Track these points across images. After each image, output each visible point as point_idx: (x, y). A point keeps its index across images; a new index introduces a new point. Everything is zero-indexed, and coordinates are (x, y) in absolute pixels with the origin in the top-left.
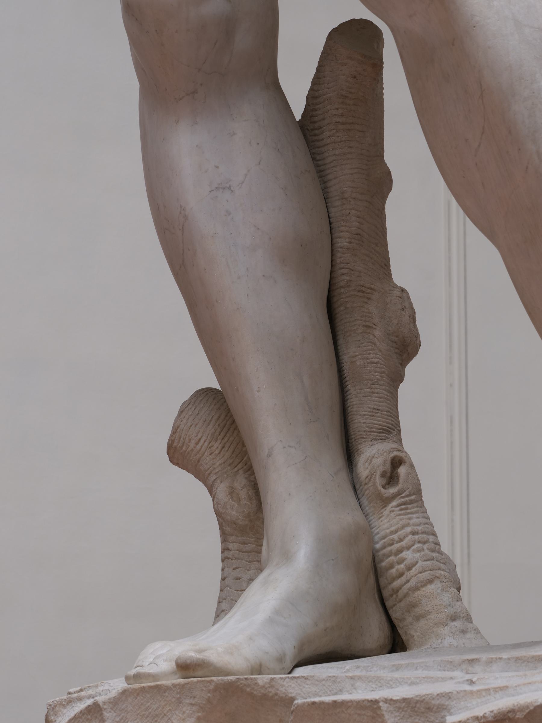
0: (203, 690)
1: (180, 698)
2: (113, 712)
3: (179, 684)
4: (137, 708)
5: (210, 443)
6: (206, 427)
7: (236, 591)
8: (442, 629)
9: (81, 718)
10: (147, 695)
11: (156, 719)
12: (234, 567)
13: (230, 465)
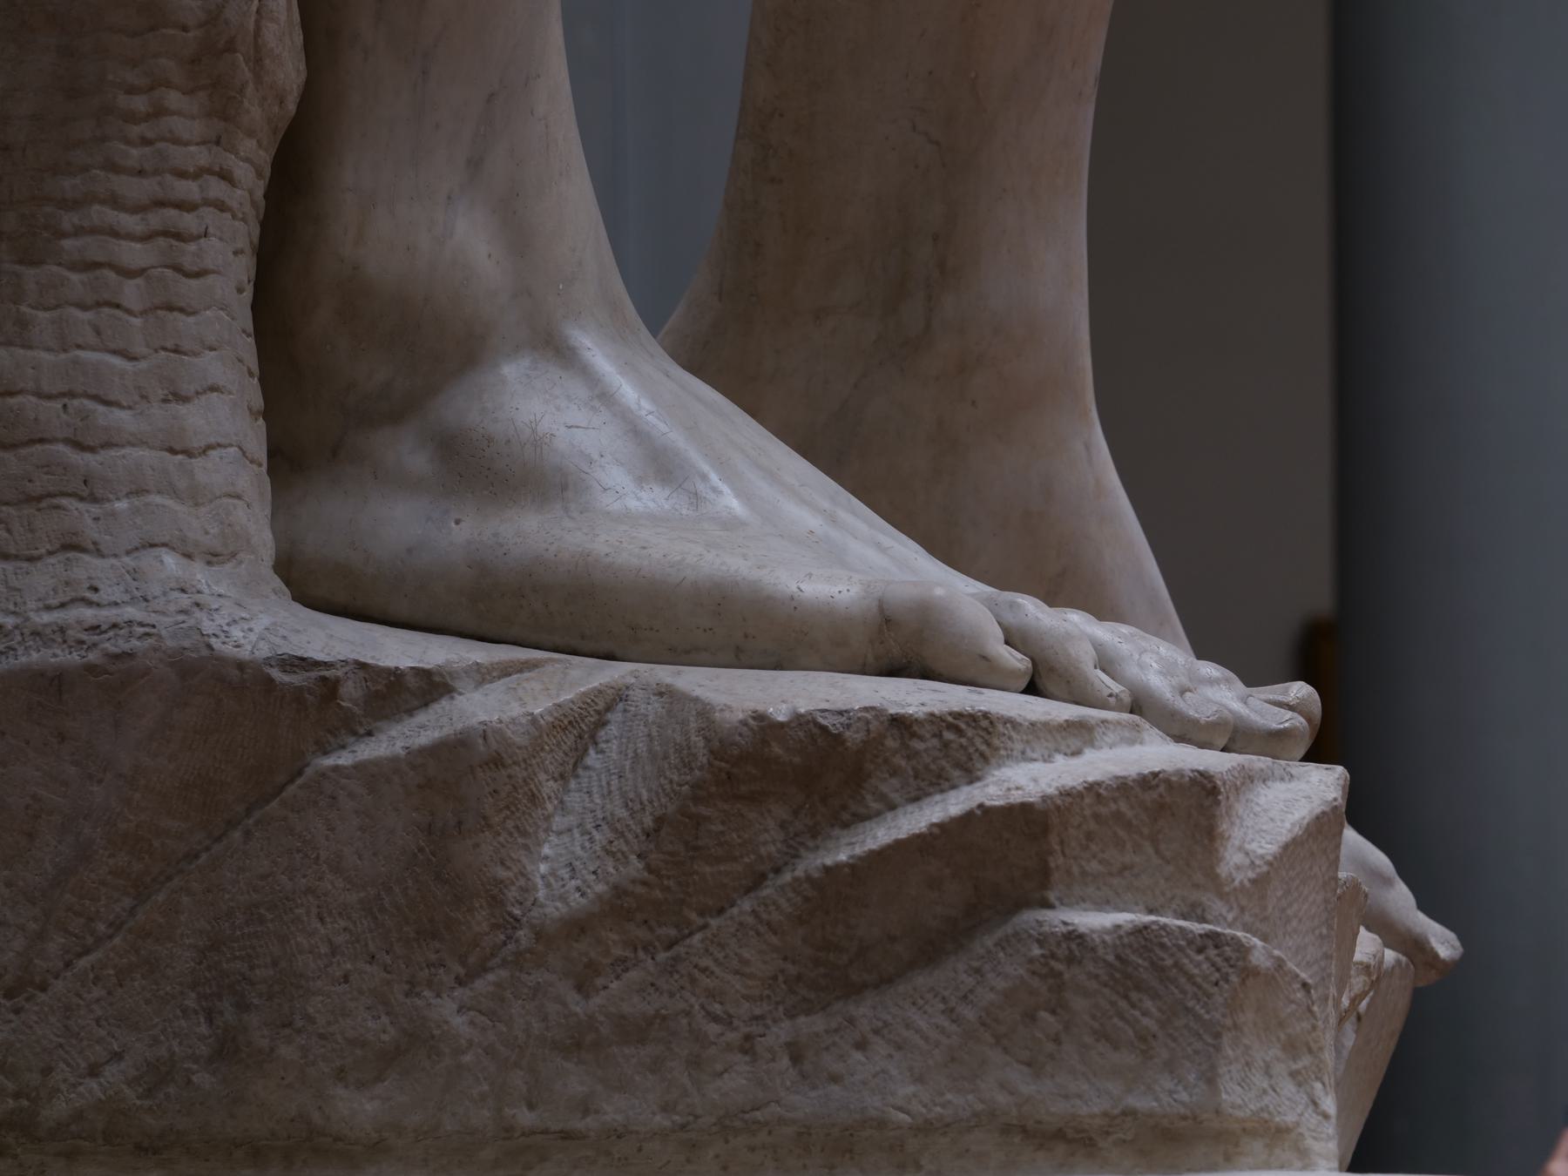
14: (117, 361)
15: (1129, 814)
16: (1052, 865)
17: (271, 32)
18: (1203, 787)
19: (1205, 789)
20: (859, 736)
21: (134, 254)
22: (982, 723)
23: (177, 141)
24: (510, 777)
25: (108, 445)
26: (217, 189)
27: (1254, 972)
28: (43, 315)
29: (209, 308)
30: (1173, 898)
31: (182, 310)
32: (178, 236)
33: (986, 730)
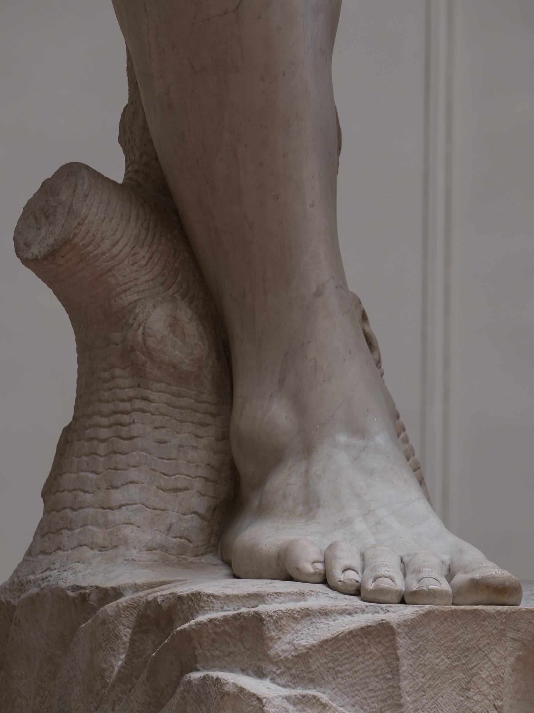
1: (504, 630)
2: (407, 638)
3: (505, 613)
5: (133, 248)
7: (161, 458)
9: (348, 640)
10: (458, 621)
11: (466, 654)
12: (157, 425)
13: (162, 284)
14: (91, 475)
15: (230, 631)
16: (197, 653)
17: (150, 342)
18: (257, 618)
21: (104, 433)
22: (196, 597)
23: (120, 388)
24: (108, 628)
25: (80, 508)
26: (138, 404)
27: (228, 694)
28: (77, 459)
29: (134, 451)
30: (251, 665)
31: (120, 453)
32: (122, 425)
33: (198, 599)
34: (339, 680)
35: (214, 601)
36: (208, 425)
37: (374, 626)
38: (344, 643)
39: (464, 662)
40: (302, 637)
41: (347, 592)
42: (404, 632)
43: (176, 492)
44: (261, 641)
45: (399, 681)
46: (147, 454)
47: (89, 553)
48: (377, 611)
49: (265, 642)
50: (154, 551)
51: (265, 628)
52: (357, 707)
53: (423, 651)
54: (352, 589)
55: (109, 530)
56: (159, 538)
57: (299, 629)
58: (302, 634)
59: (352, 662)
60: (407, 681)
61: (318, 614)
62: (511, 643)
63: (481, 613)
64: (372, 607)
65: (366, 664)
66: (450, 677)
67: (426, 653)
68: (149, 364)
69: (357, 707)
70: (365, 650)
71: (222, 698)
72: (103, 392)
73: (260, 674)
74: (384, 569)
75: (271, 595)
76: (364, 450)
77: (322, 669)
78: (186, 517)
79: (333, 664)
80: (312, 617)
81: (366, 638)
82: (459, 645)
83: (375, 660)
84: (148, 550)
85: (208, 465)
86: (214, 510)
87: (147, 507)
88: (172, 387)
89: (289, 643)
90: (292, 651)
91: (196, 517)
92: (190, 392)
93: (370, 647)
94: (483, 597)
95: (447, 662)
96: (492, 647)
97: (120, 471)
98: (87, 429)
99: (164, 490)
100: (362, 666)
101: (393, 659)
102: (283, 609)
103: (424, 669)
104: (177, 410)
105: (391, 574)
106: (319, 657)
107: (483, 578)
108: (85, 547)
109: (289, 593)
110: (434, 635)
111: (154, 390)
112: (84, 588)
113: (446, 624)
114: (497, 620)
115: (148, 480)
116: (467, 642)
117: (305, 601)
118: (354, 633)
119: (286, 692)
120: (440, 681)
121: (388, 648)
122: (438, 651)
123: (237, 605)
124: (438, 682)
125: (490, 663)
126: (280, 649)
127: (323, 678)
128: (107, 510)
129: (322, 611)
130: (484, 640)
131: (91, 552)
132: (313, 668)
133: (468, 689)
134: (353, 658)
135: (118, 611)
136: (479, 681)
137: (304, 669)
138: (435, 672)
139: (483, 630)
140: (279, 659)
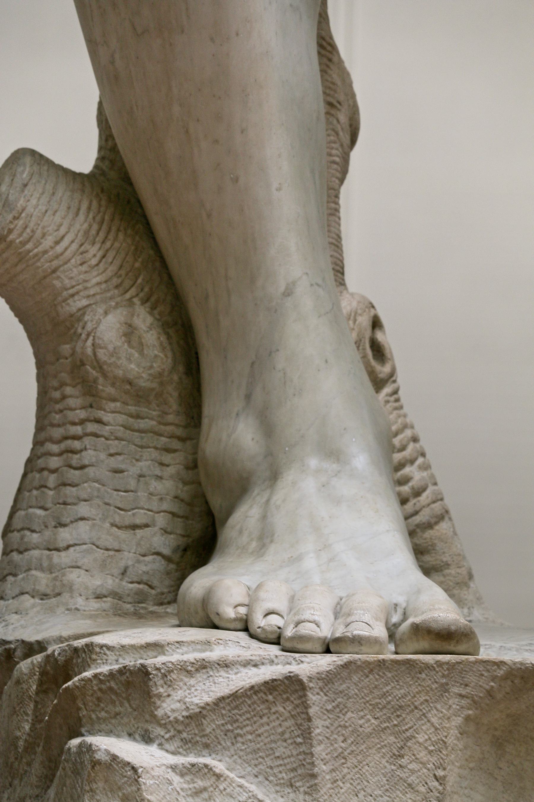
0: (482, 675)
1: (447, 684)
2: (322, 693)
3: (447, 663)
4: (366, 691)
5: (81, 245)
6: (74, 219)
7: (116, 490)
8: (466, 592)
9: (250, 697)
10: (387, 673)
11: (399, 713)
12: (112, 451)
13: (117, 287)
14: (40, 512)
15: (116, 687)
16: (81, 715)
17: (101, 354)
18: (143, 672)
19: (144, 672)
20: (63, 659)
23: (71, 409)
25: (26, 550)
26: (91, 427)
29: (86, 482)
30: (138, 728)
31: (70, 485)
32: (73, 452)
34: (239, 745)
35: (108, 652)
36: (175, 451)
37: (280, 680)
38: (245, 701)
39: (395, 722)
40: (196, 693)
41: (267, 640)
42: (318, 687)
43: (134, 530)
44: (148, 699)
45: (312, 746)
46: (100, 486)
47: (27, 601)
48: (289, 662)
49: (152, 700)
50: (105, 599)
51: (151, 683)
52: (261, 778)
53: (343, 709)
54: (273, 637)
55: (54, 575)
56: (110, 583)
57: (192, 684)
58: (196, 690)
59: (255, 723)
60: (323, 746)
61: (216, 665)
62: (457, 700)
63: (417, 664)
64: (283, 658)
65: (271, 725)
66: (377, 741)
67: (346, 712)
68: (101, 380)
69: (261, 778)
70: (270, 709)
71: (93, 767)
72: (54, 414)
73: (147, 739)
74: (308, 612)
75: (172, 644)
76: (336, 475)
77: (218, 731)
78: (146, 559)
79: (232, 725)
80: (209, 670)
81: (271, 694)
82: (389, 703)
83: (283, 721)
84: (97, 598)
85: (176, 497)
86: (185, 550)
87: (97, 547)
88: (130, 407)
89: (179, 701)
90: (183, 711)
91: (159, 558)
92: (151, 412)
93: (276, 704)
94: (425, 644)
95: (374, 724)
96: (432, 705)
97: (69, 506)
98: (39, 458)
99: (119, 528)
100: (267, 728)
101: (304, 719)
102: (173, 661)
103: (344, 732)
104: (137, 434)
105: (316, 618)
106: (215, 717)
107: (424, 622)
108: (27, 595)
109: (193, 642)
110: (356, 691)
111: (109, 410)
112: (10, 642)
113: (371, 676)
114: (437, 672)
115: (100, 516)
116: (400, 698)
117: (211, 651)
118: (256, 688)
119: (173, 760)
120: (365, 745)
121: (297, 706)
122: (362, 710)
123: (133, 657)
124: (363, 747)
125: (429, 724)
126: (169, 709)
127: (219, 743)
128: (53, 552)
129: (221, 663)
130: (420, 697)
131: (32, 601)
132: (208, 730)
133: (402, 756)
134: (255, 719)
135: (32, 668)
136: (416, 746)
137: (197, 732)
138: (358, 736)
139: (419, 685)
140: (167, 720)
